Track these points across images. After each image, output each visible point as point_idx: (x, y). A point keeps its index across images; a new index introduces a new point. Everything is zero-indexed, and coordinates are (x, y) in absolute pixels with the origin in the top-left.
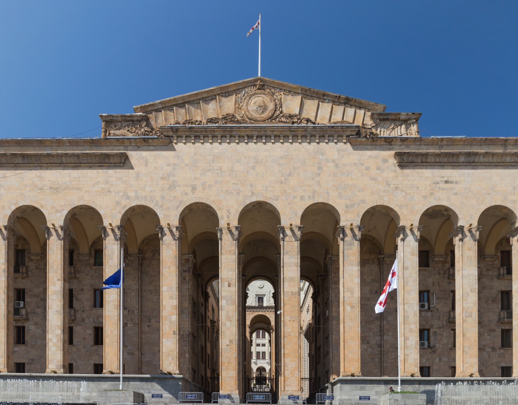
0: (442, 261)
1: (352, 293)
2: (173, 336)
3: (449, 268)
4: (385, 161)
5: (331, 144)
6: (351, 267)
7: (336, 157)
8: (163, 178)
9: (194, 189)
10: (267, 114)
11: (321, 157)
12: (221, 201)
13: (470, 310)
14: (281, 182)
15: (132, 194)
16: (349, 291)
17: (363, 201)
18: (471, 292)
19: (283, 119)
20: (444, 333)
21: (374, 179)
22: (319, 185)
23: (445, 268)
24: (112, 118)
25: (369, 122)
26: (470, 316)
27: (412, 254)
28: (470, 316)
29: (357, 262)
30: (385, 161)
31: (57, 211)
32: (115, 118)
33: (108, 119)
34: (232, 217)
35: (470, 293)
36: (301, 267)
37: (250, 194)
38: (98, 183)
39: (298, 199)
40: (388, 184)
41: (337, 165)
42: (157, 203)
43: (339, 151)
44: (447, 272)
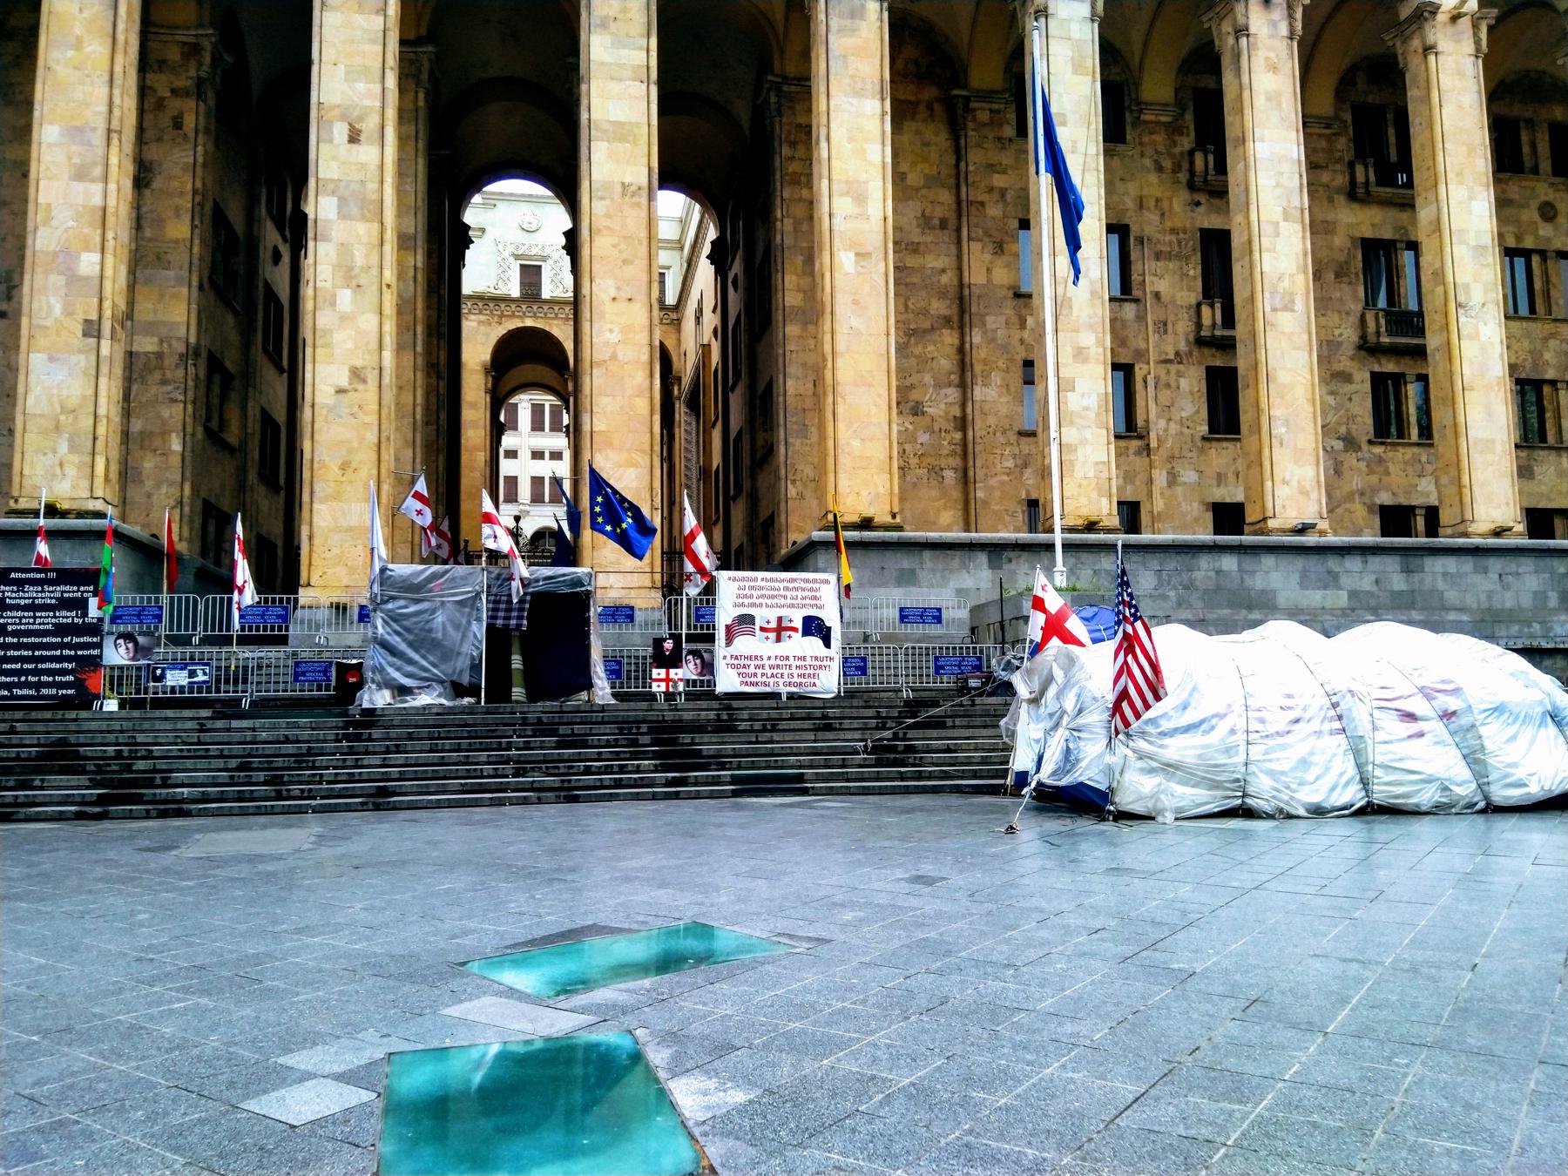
0: (1167, 124)
1: (861, 199)
3: (1191, 153)
6: (854, 101)
13: (1286, 284)
16: (847, 194)
18: (1285, 220)
20: (1183, 382)
23: (1177, 150)
26: (1285, 308)
27: (1077, 68)
28: (1289, 307)
29: (877, 81)
35: (1283, 224)
36: (661, 83)
44: (1186, 166)
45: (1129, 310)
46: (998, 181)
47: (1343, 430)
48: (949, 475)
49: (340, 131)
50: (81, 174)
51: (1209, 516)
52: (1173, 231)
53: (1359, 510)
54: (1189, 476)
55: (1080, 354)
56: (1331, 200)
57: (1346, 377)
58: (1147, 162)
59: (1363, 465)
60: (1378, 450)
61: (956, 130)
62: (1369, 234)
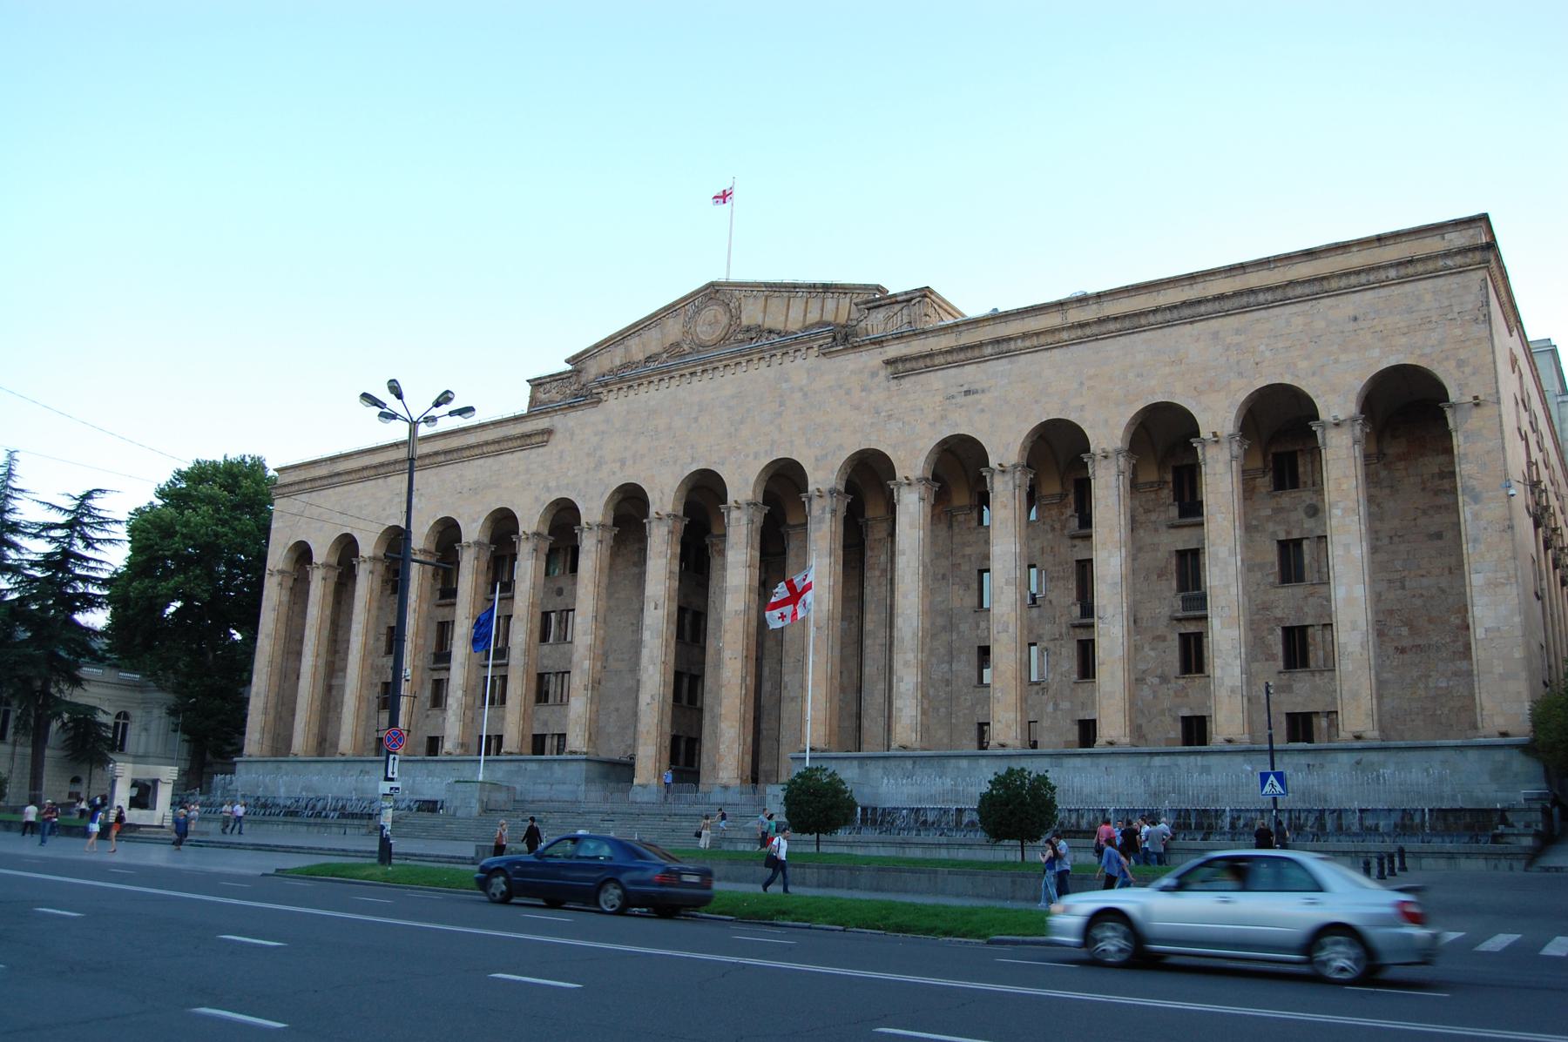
4: (874, 374)
5: (799, 361)
8: (589, 455)
9: (623, 463)
10: (719, 332)
11: (784, 386)
14: (730, 435)
15: (552, 484)
17: (840, 447)
19: (740, 336)
21: (857, 408)
22: (781, 431)
25: (855, 315)
30: (874, 374)
31: (474, 521)
34: (665, 499)
41: (805, 395)
43: (808, 371)
45: (1035, 612)
46: (968, 551)
47: (1159, 672)
48: (943, 710)
49: (652, 605)
50: (585, 634)
51: (1076, 728)
52: (1060, 564)
53: (1168, 720)
54: (1065, 705)
55: (906, 664)
56: (1156, 530)
57: (1163, 638)
58: (1047, 527)
59: (1171, 692)
60: (1181, 682)
61: (950, 526)
62: (1181, 547)
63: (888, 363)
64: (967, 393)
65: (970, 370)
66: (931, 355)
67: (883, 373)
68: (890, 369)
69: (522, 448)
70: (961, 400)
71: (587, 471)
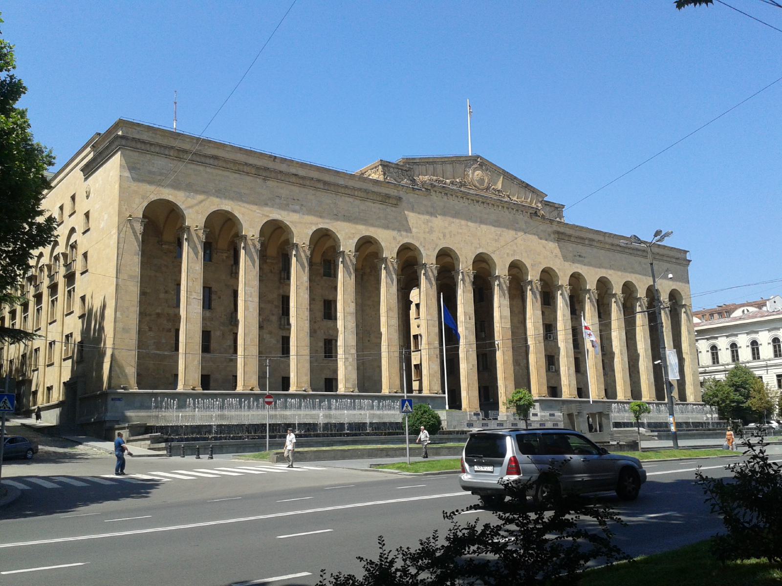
2: (435, 359)
7: (524, 227)
12: (461, 248)
24: (388, 164)
32: (390, 165)
33: (386, 164)
37: (478, 246)
38: (379, 218)
39: (506, 256)
40: (552, 253)
42: (421, 242)
63: (558, 233)
64: (580, 256)
65: (580, 246)
66: (570, 236)
67: (552, 236)
68: (556, 236)
69: (382, 202)
70: (578, 258)
71: (424, 232)
